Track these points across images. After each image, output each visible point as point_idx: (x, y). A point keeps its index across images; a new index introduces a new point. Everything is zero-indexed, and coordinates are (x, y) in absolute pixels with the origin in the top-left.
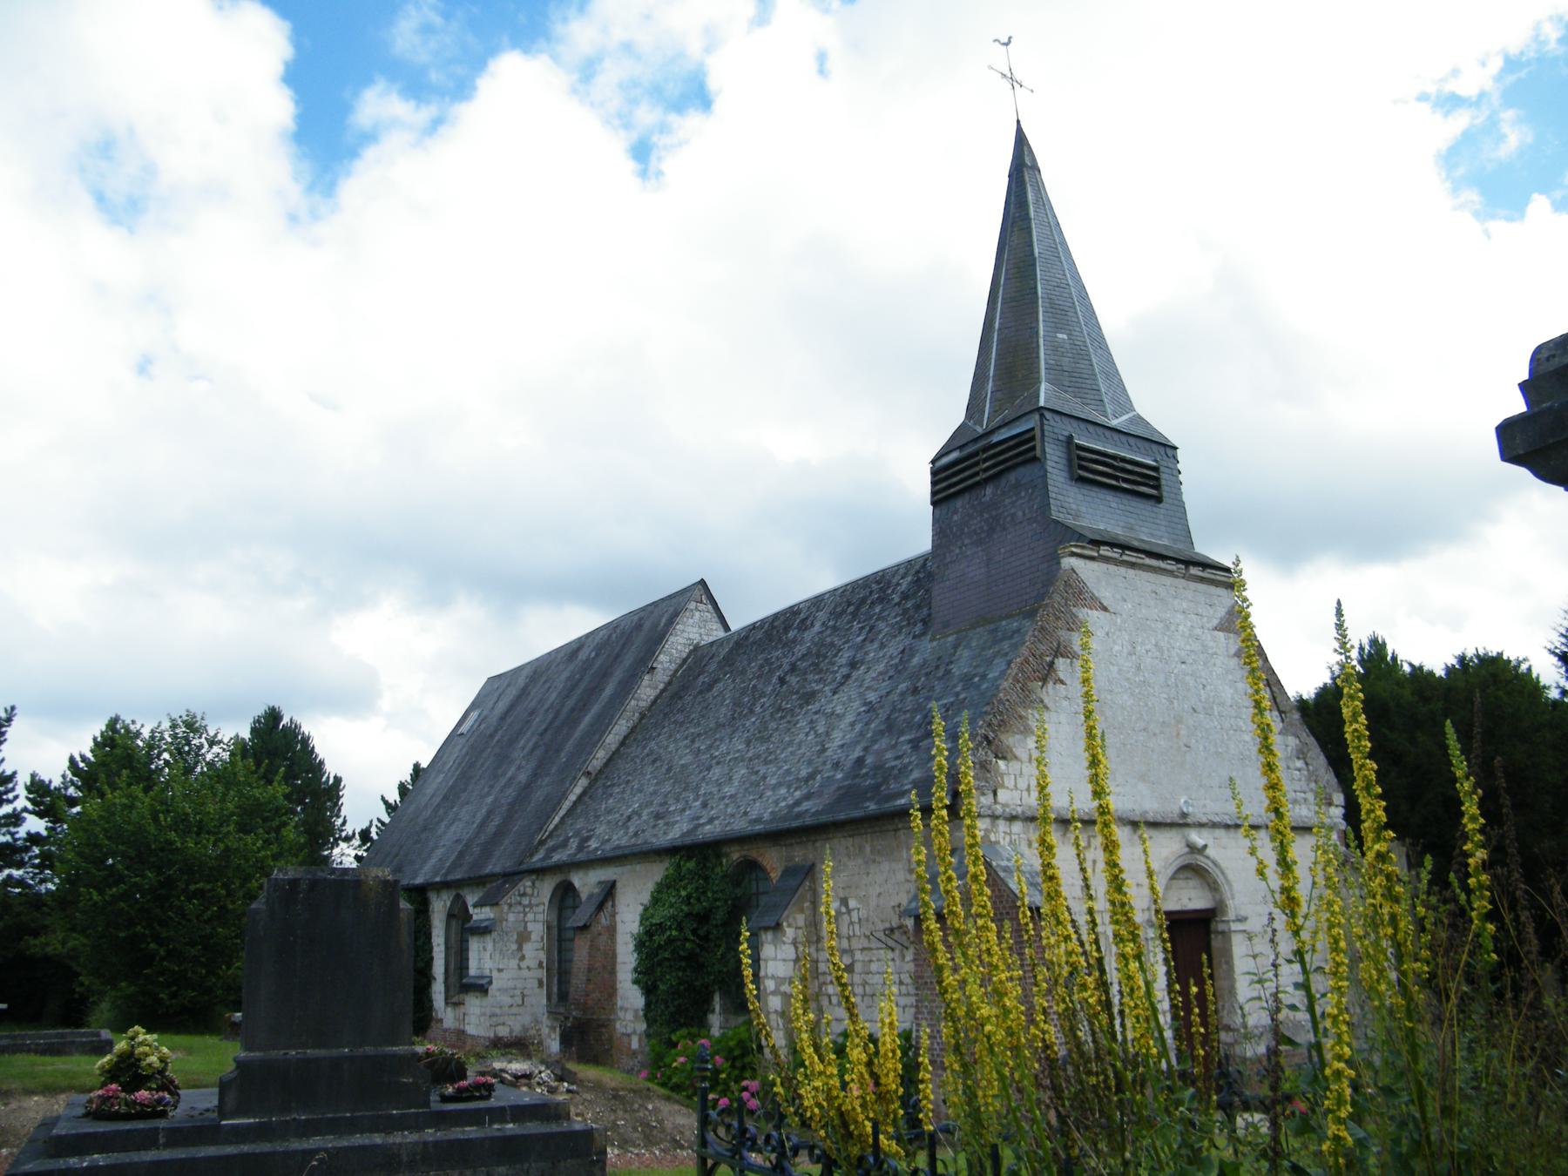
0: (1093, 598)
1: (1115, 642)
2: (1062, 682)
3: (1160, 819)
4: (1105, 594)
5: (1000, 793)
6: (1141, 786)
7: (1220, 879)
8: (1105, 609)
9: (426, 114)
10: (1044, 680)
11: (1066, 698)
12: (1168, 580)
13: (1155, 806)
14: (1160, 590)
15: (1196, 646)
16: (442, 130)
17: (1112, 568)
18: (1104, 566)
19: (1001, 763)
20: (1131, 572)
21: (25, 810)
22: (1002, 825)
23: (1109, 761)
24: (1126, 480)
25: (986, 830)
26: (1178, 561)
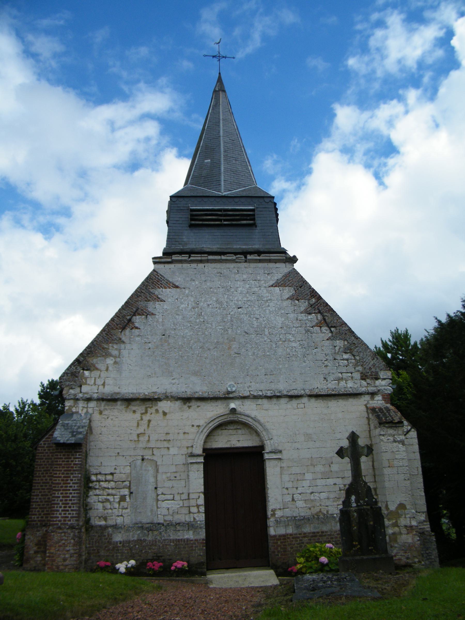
0: (168, 282)
1: (182, 303)
2: (137, 328)
3: (206, 395)
4: (178, 279)
5: (83, 387)
6: (193, 379)
7: (259, 428)
8: (177, 287)
9: (295, 184)
10: (124, 328)
11: (139, 336)
12: (232, 265)
13: (205, 389)
14: (225, 272)
15: (253, 298)
16: (303, 188)
17: (185, 265)
18: (179, 265)
19: (87, 373)
20: (201, 265)
21: (65, 569)
22: (81, 404)
23: (282, 386)
24: (225, 220)
25: (70, 406)
26: (236, 254)
